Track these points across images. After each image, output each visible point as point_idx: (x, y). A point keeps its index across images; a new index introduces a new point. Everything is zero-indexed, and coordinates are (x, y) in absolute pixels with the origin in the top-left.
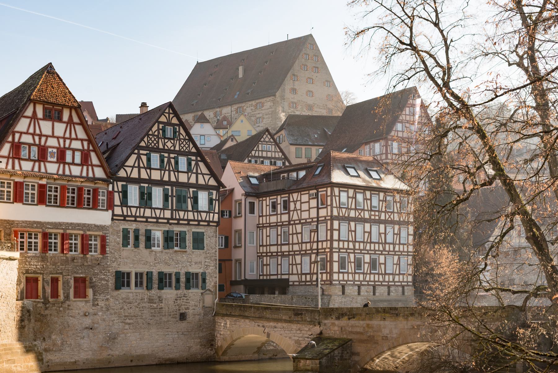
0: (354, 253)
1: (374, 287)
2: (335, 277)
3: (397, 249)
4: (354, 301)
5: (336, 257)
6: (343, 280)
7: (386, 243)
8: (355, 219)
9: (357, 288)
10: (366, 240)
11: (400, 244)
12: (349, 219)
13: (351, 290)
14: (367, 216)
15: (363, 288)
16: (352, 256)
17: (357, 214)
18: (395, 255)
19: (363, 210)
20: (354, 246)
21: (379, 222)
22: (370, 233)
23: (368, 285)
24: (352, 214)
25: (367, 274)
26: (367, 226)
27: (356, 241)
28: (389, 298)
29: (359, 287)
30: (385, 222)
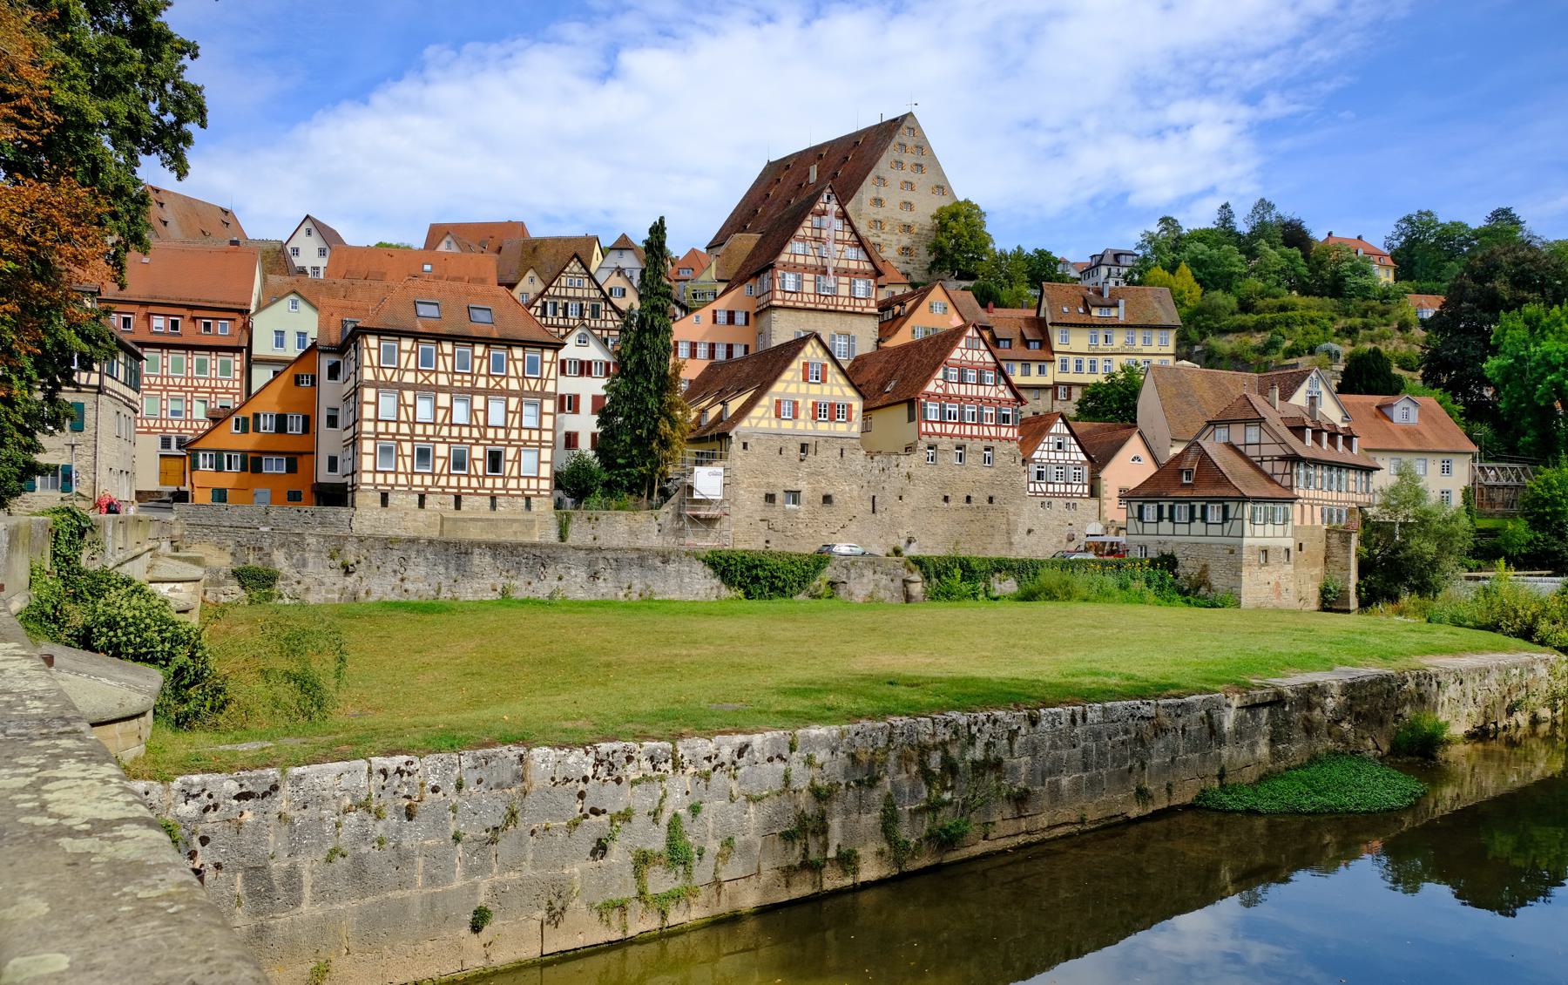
0: (412, 441)
1: (458, 499)
2: (367, 478)
3: (514, 435)
4: (409, 518)
5: (368, 446)
6: (385, 484)
7: (487, 426)
8: (413, 387)
9: (416, 497)
10: (439, 420)
11: (521, 428)
12: (401, 387)
13: (403, 502)
14: (443, 380)
15: (429, 499)
16: (407, 448)
17: (420, 378)
18: (510, 445)
19: (436, 372)
20: (412, 430)
21: (474, 391)
22: (450, 410)
23: (444, 493)
24: (409, 378)
25: (440, 475)
26: (444, 399)
27: (415, 422)
28: (493, 515)
29: (422, 498)
30: (487, 392)
